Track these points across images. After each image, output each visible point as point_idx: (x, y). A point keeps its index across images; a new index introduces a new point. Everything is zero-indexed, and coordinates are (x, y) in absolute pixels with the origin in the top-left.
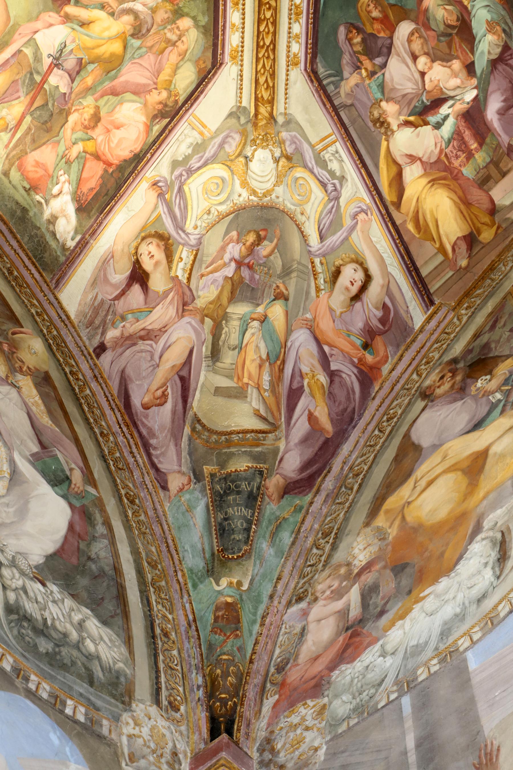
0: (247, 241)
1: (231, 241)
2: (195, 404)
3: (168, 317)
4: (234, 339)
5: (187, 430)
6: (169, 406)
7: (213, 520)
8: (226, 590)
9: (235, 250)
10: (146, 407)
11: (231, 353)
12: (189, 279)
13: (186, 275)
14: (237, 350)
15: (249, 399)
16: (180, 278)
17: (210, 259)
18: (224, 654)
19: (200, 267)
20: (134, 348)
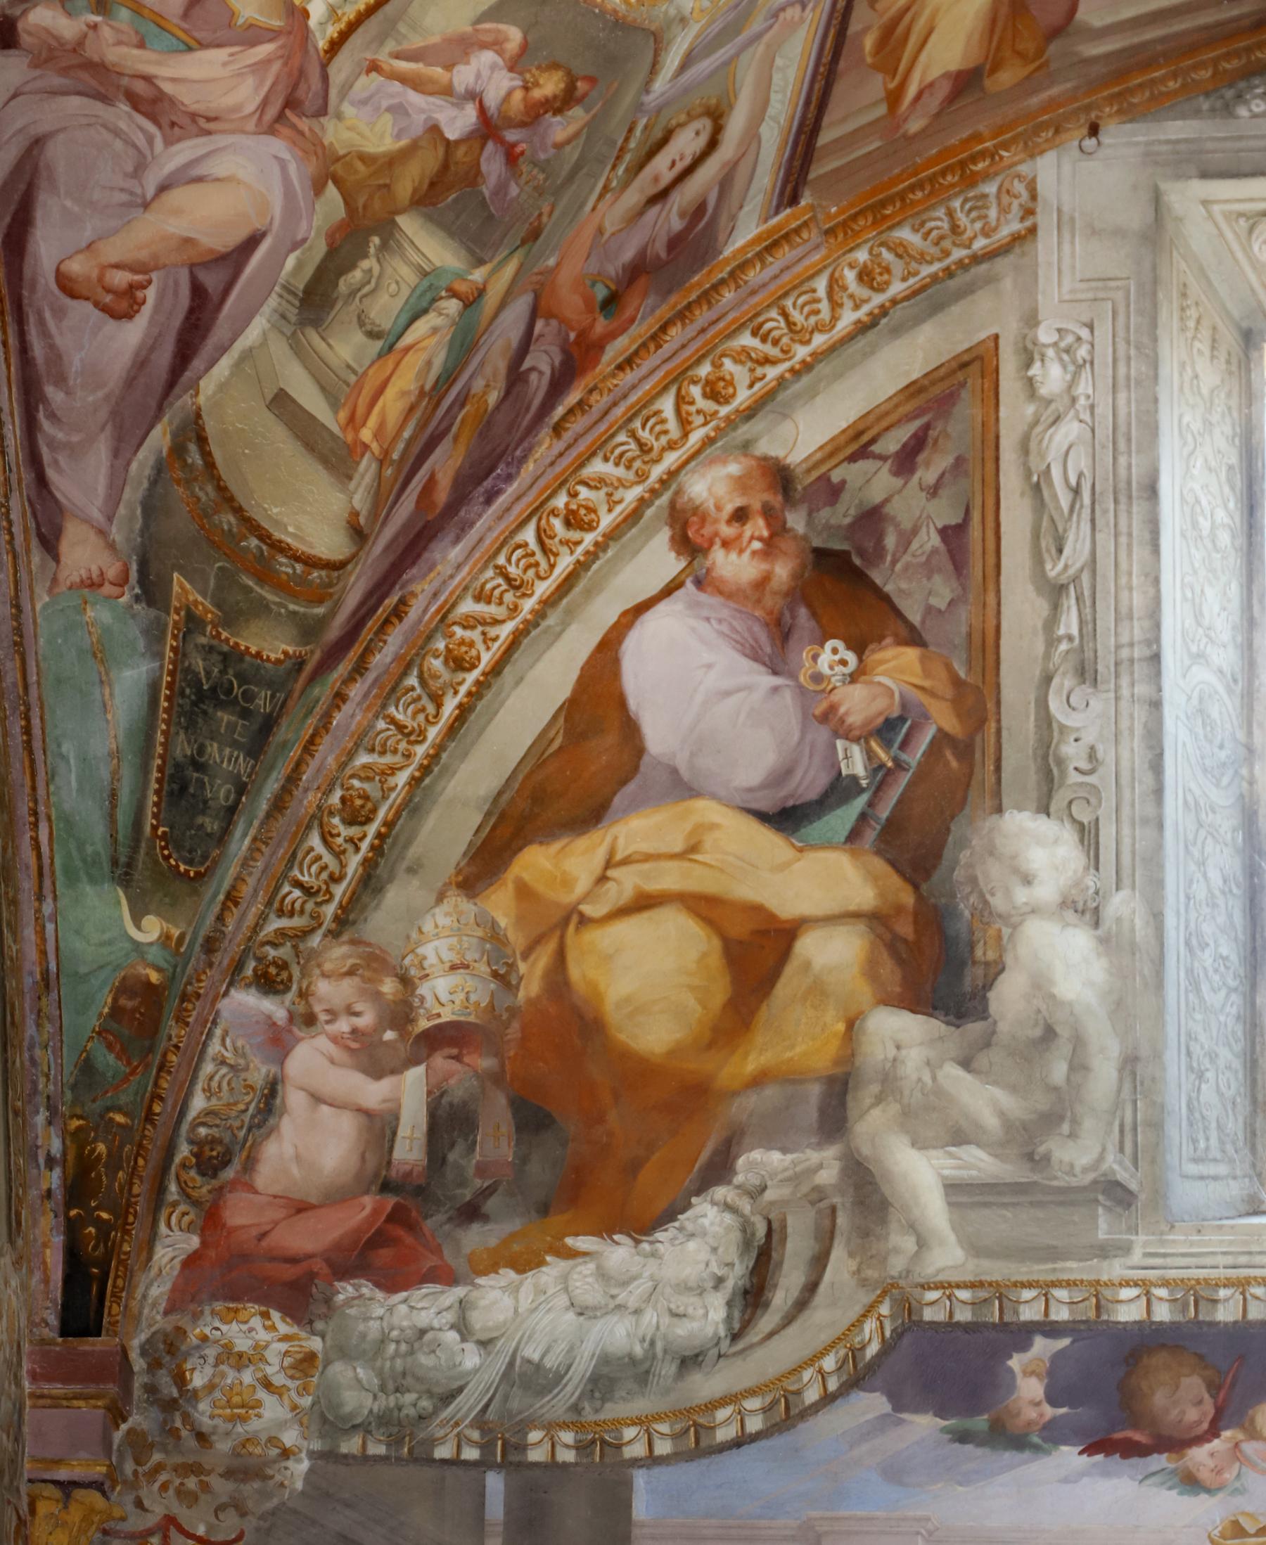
0: (537, 84)
1: (496, 45)
2: (208, 385)
3: (229, 101)
4: (384, 310)
5: (160, 438)
6: (133, 333)
7: (160, 738)
8: (154, 949)
9: (490, 77)
10: (67, 285)
11: (359, 337)
12: (335, 46)
13: (332, 31)
14: (379, 344)
15: (352, 485)
16: (313, 23)
17: (416, 42)
18: (119, 1110)
19: (381, 39)
20: (98, 107)
